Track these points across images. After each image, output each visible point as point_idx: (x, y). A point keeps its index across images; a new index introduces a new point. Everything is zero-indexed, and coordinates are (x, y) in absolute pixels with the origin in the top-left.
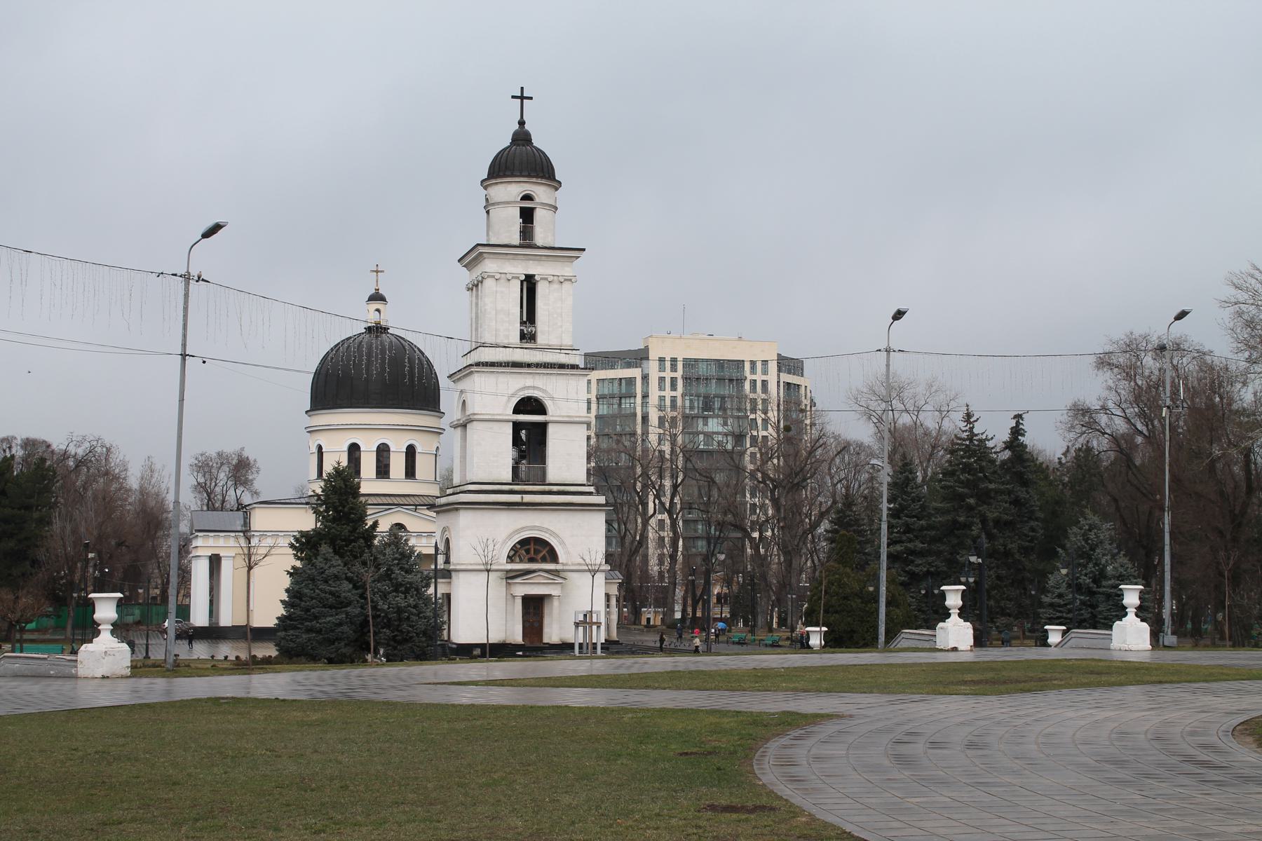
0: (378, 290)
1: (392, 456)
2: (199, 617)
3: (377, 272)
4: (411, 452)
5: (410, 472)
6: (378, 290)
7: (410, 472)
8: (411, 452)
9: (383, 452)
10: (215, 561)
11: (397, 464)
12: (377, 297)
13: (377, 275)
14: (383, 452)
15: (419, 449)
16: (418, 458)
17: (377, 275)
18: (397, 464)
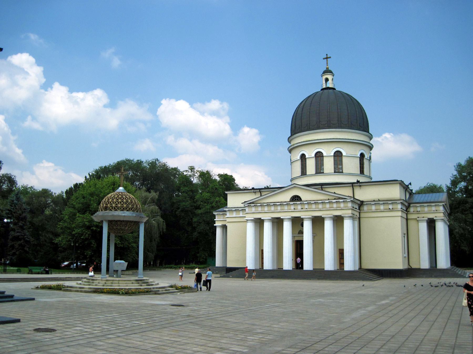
0: (328, 68)
1: (325, 159)
2: (218, 262)
3: (327, 58)
4: (338, 155)
5: (338, 169)
6: (328, 68)
7: (338, 169)
8: (338, 155)
9: (319, 156)
10: (224, 227)
11: (329, 164)
12: (328, 71)
13: (327, 61)
14: (319, 156)
15: (344, 154)
16: (345, 160)
17: (327, 61)
18: (329, 164)
